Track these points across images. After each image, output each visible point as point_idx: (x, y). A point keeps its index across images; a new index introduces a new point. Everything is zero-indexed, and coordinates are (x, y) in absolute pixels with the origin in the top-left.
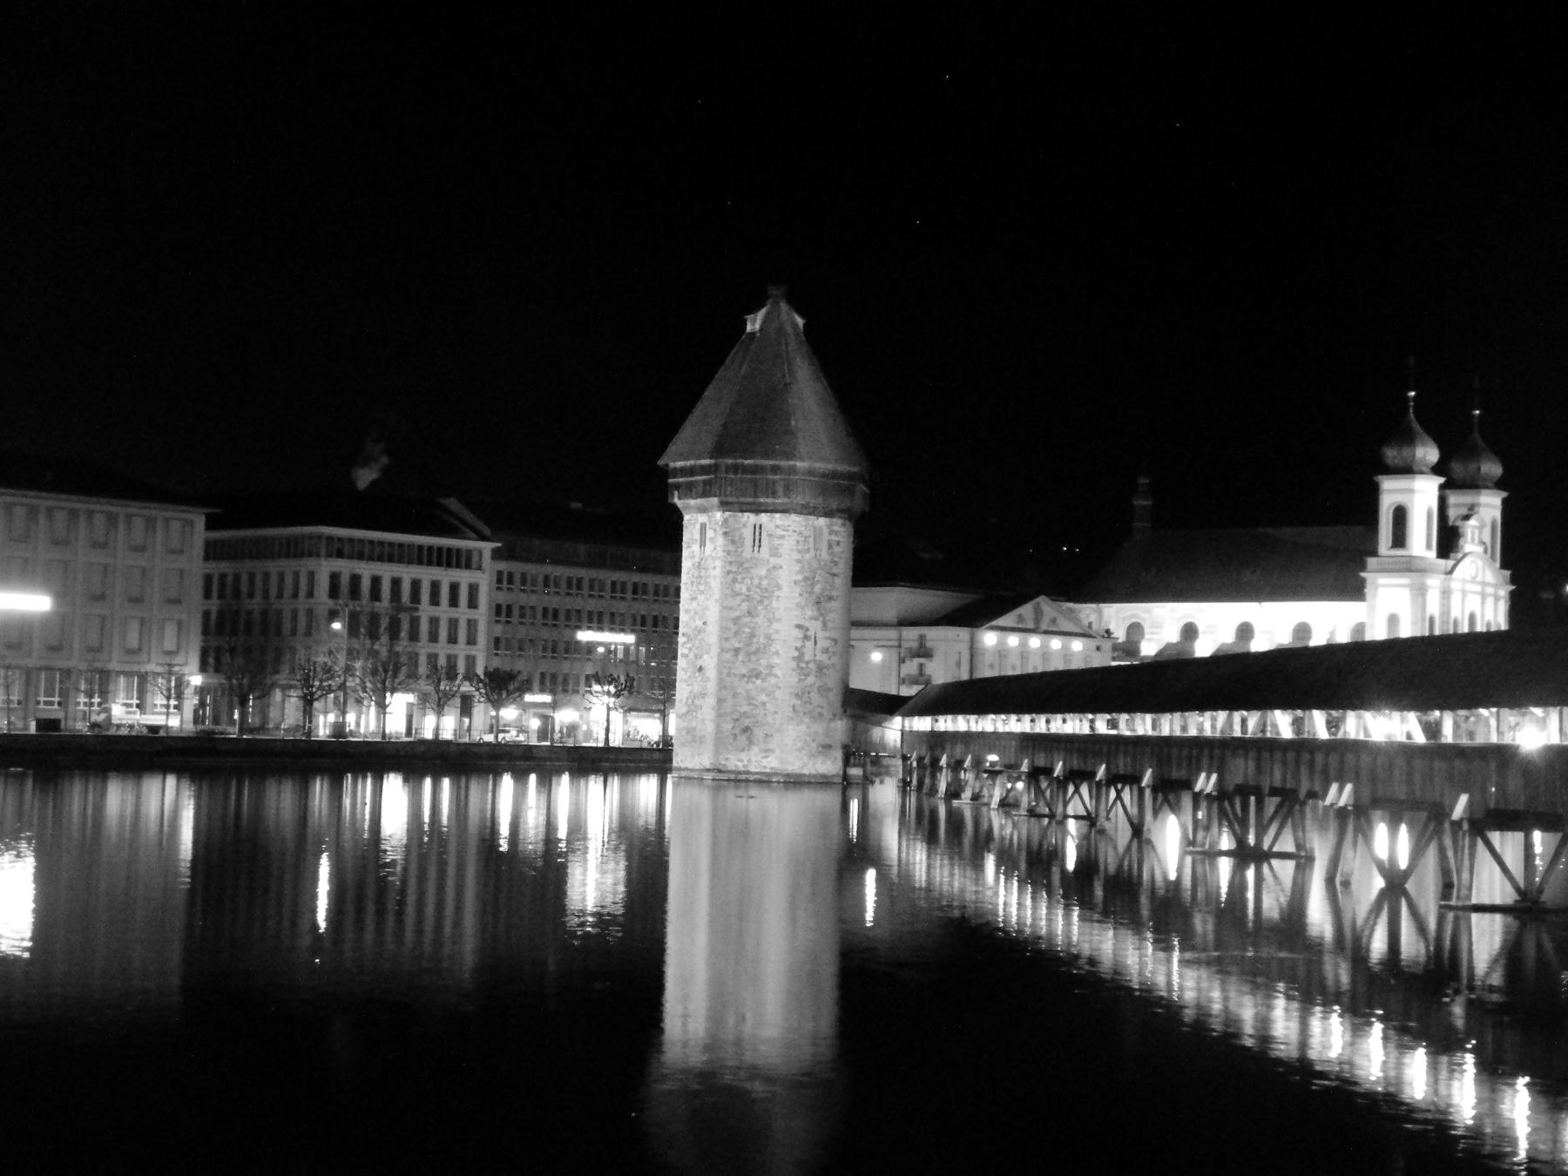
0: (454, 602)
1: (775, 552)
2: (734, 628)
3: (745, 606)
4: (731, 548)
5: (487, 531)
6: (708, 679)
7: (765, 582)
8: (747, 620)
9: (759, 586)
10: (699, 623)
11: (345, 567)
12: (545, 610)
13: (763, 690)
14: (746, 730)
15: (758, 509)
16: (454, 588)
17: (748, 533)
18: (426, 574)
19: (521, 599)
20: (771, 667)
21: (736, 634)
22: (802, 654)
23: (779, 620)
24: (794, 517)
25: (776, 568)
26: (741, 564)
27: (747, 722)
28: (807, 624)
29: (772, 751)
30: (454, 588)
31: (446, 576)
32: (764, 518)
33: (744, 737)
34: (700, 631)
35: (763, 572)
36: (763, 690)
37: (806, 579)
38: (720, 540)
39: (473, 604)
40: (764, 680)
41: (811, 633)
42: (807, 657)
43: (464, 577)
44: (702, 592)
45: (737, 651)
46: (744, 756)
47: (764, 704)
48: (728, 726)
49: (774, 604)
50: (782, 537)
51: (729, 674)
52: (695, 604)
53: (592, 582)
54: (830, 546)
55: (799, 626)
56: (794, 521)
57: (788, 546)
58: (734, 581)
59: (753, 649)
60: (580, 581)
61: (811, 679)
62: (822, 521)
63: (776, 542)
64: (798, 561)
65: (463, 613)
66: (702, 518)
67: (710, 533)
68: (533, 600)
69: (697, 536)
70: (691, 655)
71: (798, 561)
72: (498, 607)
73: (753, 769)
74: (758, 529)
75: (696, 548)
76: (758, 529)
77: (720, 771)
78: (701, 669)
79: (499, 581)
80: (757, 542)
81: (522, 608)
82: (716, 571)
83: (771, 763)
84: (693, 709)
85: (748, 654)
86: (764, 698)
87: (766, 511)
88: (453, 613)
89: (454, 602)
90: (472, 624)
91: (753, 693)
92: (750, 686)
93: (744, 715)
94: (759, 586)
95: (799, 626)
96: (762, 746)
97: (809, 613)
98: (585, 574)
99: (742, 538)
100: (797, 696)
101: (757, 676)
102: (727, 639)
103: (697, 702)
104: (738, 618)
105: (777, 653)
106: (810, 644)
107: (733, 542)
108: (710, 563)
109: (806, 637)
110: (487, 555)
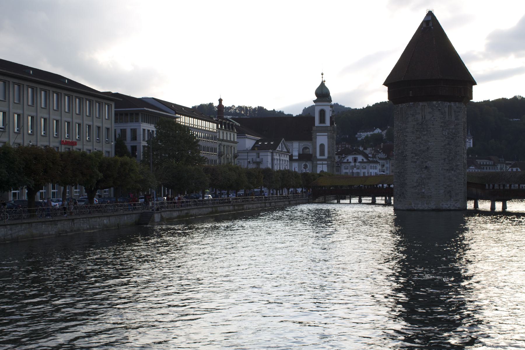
4: (442, 116)
8: (448, 146)
15: (450, 102)
17: (447, 109)
20: (457, 165)
32: (452, 104)
44: (424, 135)
45: (444, 159)
47: (455, 181)
50: (459, 112)
59: (450, 158)
66: (421, 104)
73: (452, 208)
74: (450, 107)
76: (450, 107)
78: (426, 167)
101: (452, 169)
102: (441, 154)
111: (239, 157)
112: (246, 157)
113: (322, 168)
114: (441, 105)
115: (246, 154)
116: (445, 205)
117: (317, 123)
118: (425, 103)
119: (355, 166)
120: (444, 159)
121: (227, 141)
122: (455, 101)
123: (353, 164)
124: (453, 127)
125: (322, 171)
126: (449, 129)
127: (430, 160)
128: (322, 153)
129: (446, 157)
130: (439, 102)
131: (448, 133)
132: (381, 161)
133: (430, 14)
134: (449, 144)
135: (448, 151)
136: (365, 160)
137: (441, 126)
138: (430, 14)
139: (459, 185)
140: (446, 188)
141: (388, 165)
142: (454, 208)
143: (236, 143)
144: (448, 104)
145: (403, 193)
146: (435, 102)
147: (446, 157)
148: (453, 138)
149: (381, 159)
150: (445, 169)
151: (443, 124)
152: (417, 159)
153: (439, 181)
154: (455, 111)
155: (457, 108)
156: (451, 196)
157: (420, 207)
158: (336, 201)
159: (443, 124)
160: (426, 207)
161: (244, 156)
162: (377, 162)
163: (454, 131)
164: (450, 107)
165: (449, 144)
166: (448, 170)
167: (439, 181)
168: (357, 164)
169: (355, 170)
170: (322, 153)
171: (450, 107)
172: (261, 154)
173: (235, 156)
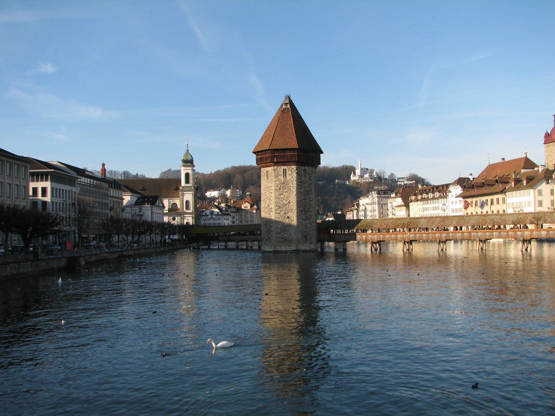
10: (284, 202)
15: (305, 166)
17: (302, 172)
20: (311, 216)
27: (305, 234)
29: (312, 243)
32: (307, 168)
35: (307, 185)
40: (309, 220)
45: (302, 211)
48: (300, 236)
66: (283, 167)
78: (288, 217)
85: (305, 212)
92: (306, 222)
104: (302, 200)
111: (125, 211)
113: (189, 220)
116: (303, 247)
117: (183, 183)
118: (286, 167)
119: (212, 218)
120: (302, 211)
121: (116, 198)
122: (308, 165)
123: (210, 217)
125: (187, 223)
128: (187, 208)
132: (232, 214)
134: (305, 199)
136: (220, 213)
141: (237, 217)
145: (269, 238)
149: (232, 212)
156: (306, 239)
157: (283, 249)
158: (206, 247)
160: (288, 249)
161: (128, 210)
162: (229, 215)
164: (305, 171)
165: (305, 199)
168: (214, 216)
169: (212, 222)
170: (187, 208)
171: (305, 171)
172: (143, 208)
173: (123, 210)
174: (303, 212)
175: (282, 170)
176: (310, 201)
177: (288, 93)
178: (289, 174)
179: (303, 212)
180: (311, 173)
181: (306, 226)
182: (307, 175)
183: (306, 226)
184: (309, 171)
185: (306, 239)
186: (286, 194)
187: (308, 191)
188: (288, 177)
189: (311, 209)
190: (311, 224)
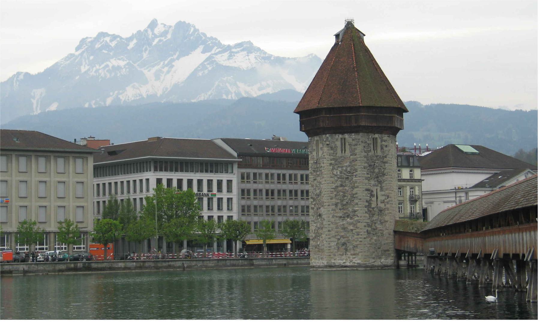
0: (220, 189)
1: (353, 153)
2: (335, 193)
3: (339, 183)
4: (332, 151)
5: (235, 154)
6: (324, 219)
7: (349, 169)
8: (340, 188)
9: (346, 170)
10: (318, 191)
11: (165, 176)
12: (267, 191)
13: (351, 224)
14: (344, 244)
15: (343, 133)
16: (220, 183)
17: (338, 144)
18: (205, 177)
19: (252, 186)
21: (336, 195)
22: (370, 204)
23: (357, 187)
24: (361, 134)
25: (355, 160)
26: (335, 160)
27: (343, 240)
28: (372, 188)
29: (358, 254)
30: (220, 183)
31: (215, 177)
32: (346, 136)
33: (344, 247)
34: (318, 195)
36: (351, 224)
37: (370, 166)
38: (326, 149)
39: (229, 190)
40: (351, 218)
41: (375, 193)
42: (373, 206)
43: (224, 177)
44: (318, 176)
45: (336, 205)
46: (344, 257)
47: (352, 230)
48: (333, 244)
49: (354, 179)
50: (356, 145)
51: (333, 217)
52: (315, 182)
53: (290, 176)
54: (382, 148)
55: (367, 190)
56: (361, 137)
57: (359, 149)
58: (333, 169)
60: (284, 175)
61: (375, 218)
62: (376, 136)
63: (353, 147)
64: (365, 157)
65: (225, 195)
66: (316, 138)
67: (321, 146)
68: (260, 186)
69: (315, 148)
70: (315, 208)
71: (365, 157)
72: (243, 191)
73: (348, 264)
74: (343, 141)
75: (314, 153)
76: (343, 141)
77: (331, 266)
79: (243, 178)
80: (343, 149)
81: (255, 191)
82: (325, 164)
83: (357, 261)
84: (318, 235)
86: (351, 227)
87: (347, 133)
88: (219, 196)
89: (220, 189)
90: (229, 200)
91: (346, 226)
92: (344, 222)
93: (342, 236)
94: (346, 170)
95: (367, 190)
96: (352, 253)
97: (373, 182)
98: (287, 172)
99: (336, 147)
100: (369, 226)
101: (348, 216)
102: (331, 199)
103: (320, 231)
104: (337, 187)
105: (357, 204)
106: (374, 199)
107: (332, 148)
108: (321, 160)
109: (372, 195)
110: (235, 166)
112: (454, 199)
114: (330, 138)
115: (454, 195)
116: (339, 261)
120: (336, 205)
124: (348, 164)
126: (343, 167)
127: (322, 206)
129: (339, 201)
130: (328, 135)
131: (341, 172)
133: (349, 26)
134: (342, 186)
135: (341, 193)
137: (331, 164)
138: (349, 26)
139: (358, 235)
140: (339, 239)
142: (351, 264)
143: (420, 181)
144: (341, 136)
146: (324, 136)
147: (339, 201)
148: (347, 178)
150: (337, 217)
151: (333, 162)
152: (315, 204)
153: (329, 231)
154: (350, 145)
155: (353, 140)
156: (346, 250)
159: (333, 162)
163: (349, 169)
165: (342, 186)
166: (341, 217)
167: (329, 231)
174: (340, 206)
175: (315, 142)
176: (353, 188)
177: (349, 18)
178: (321, 148)
179: (340, 206)
180: (354, 143)
181: (344, 229)
182: (347, 147)
183: (344, 229)
184: (350, 140)
185: (346, 250)
186: (318, 179)
187: (350, 172)
188: (320, 153)
189: (356, 201)
190: (354, 225)
